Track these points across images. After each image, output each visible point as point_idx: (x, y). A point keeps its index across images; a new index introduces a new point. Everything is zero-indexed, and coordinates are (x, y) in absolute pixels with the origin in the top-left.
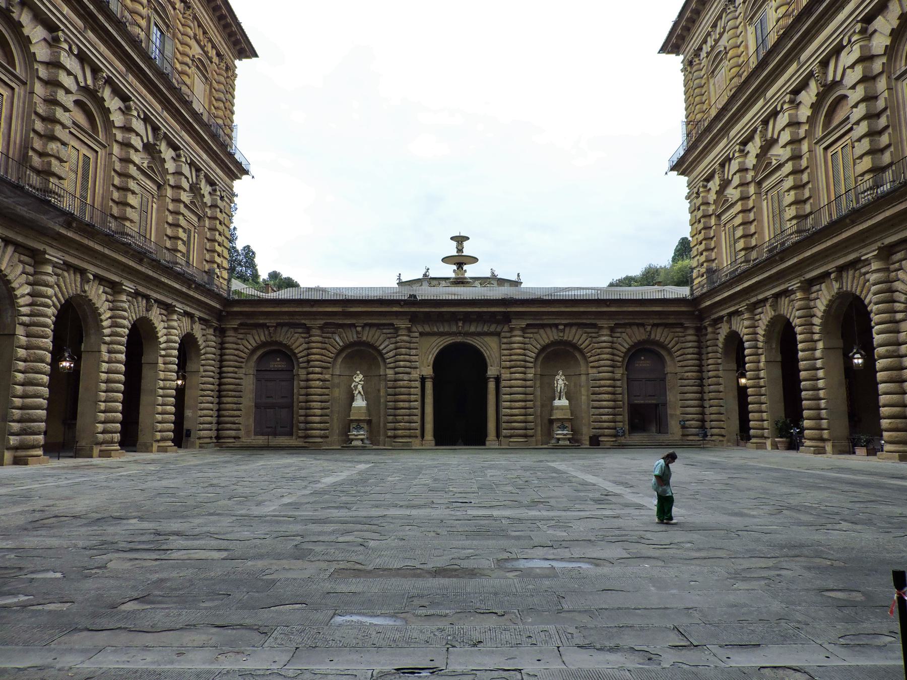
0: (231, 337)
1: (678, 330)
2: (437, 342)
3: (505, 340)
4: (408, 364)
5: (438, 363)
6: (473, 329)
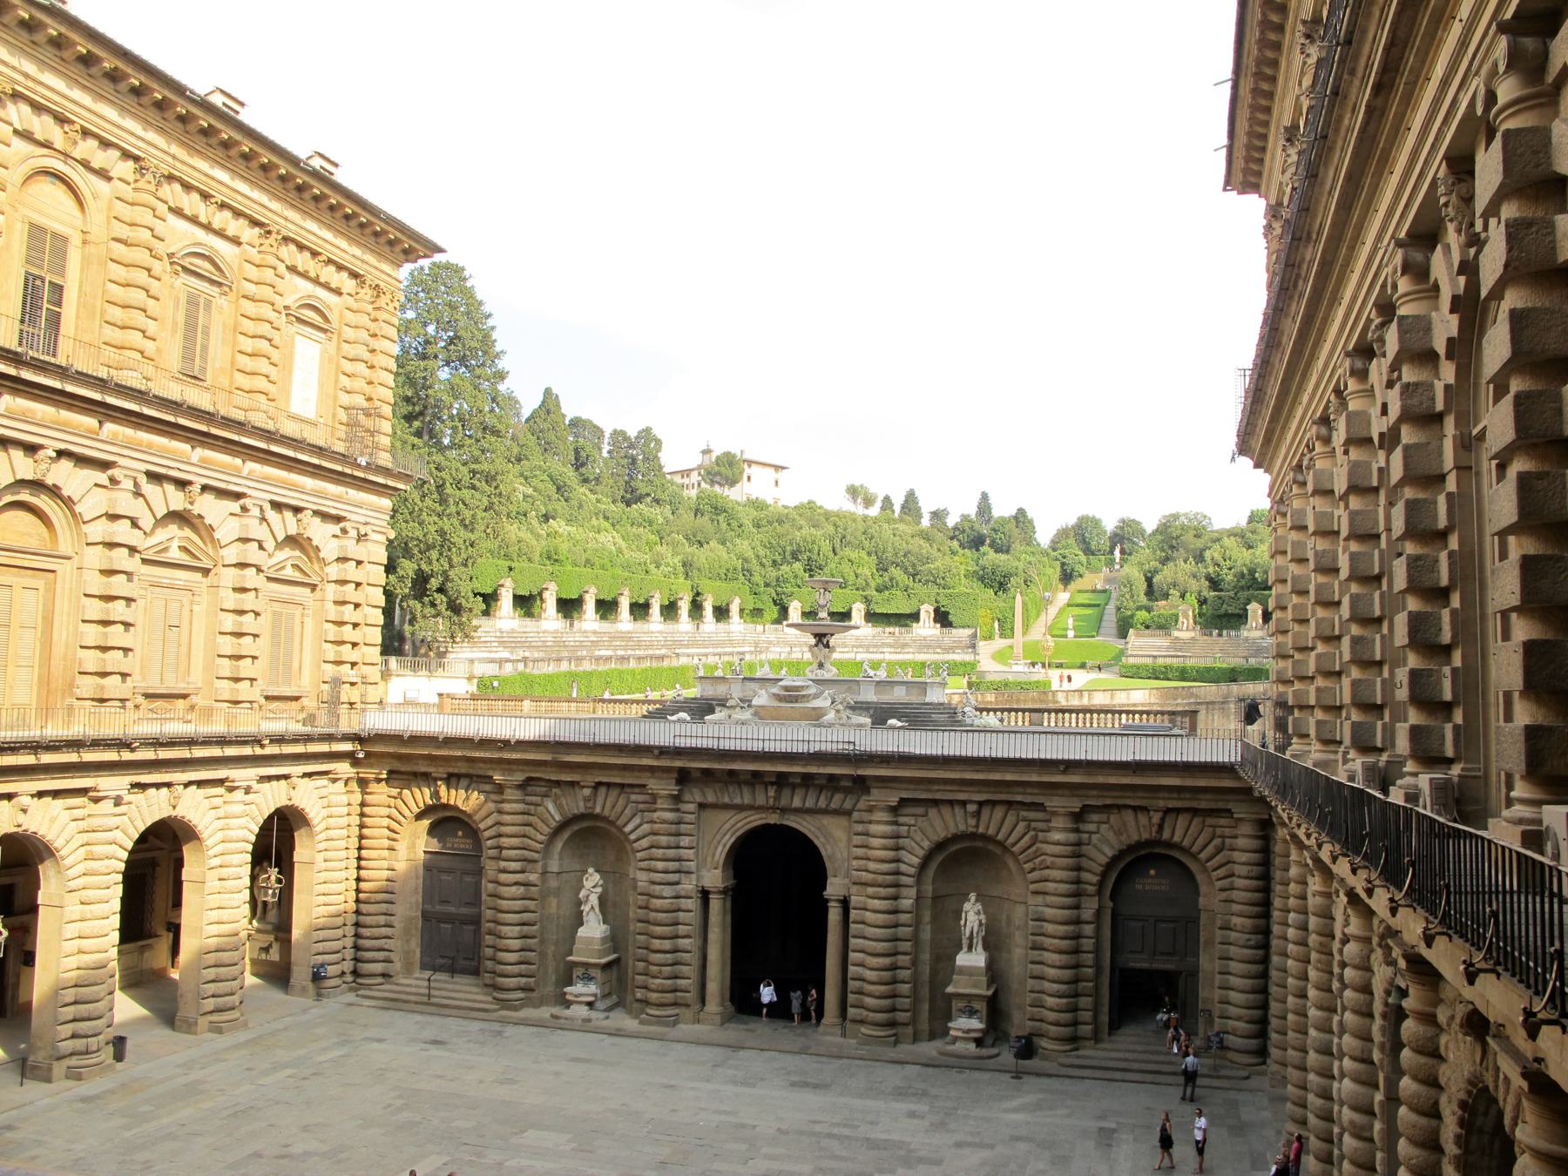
1: (1222, 821)
2: (732, 822)
3: (859, 828)
4: (672, 865)
6: (797, 803)
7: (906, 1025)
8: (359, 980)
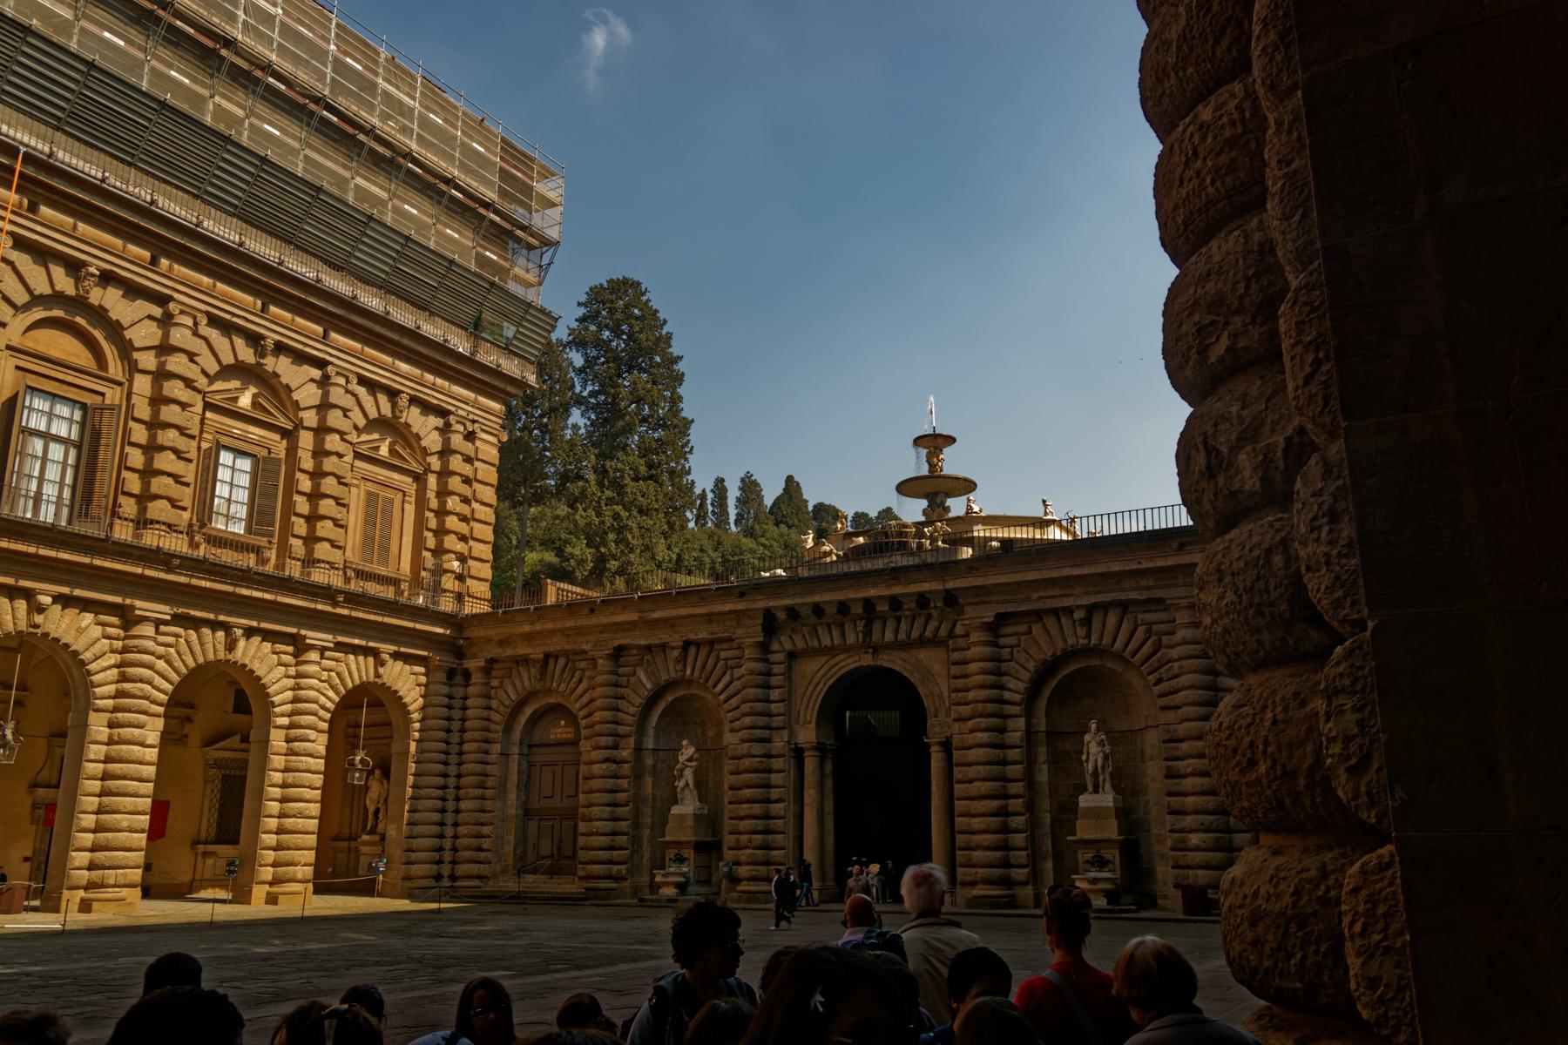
3: (956, 656)
4: (760, 720)
7: (1025, 883)
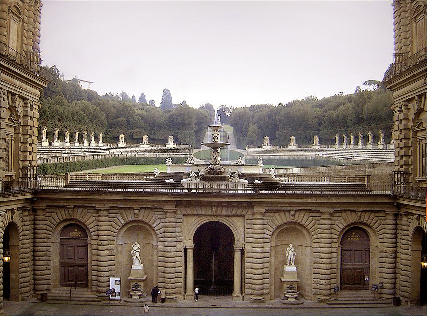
0: (41, 216)
1: (381, 214)
3: (248, 221)
4: (174, 239)
5: (199, 236)
8: (36, 293)
